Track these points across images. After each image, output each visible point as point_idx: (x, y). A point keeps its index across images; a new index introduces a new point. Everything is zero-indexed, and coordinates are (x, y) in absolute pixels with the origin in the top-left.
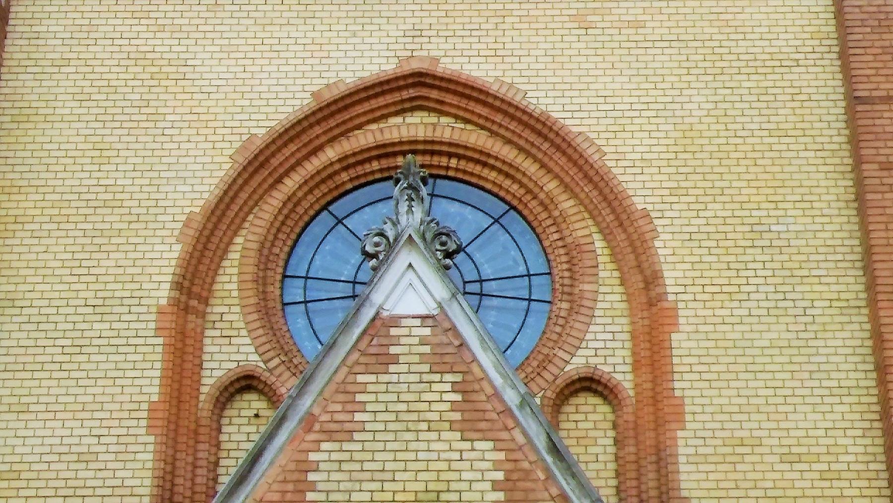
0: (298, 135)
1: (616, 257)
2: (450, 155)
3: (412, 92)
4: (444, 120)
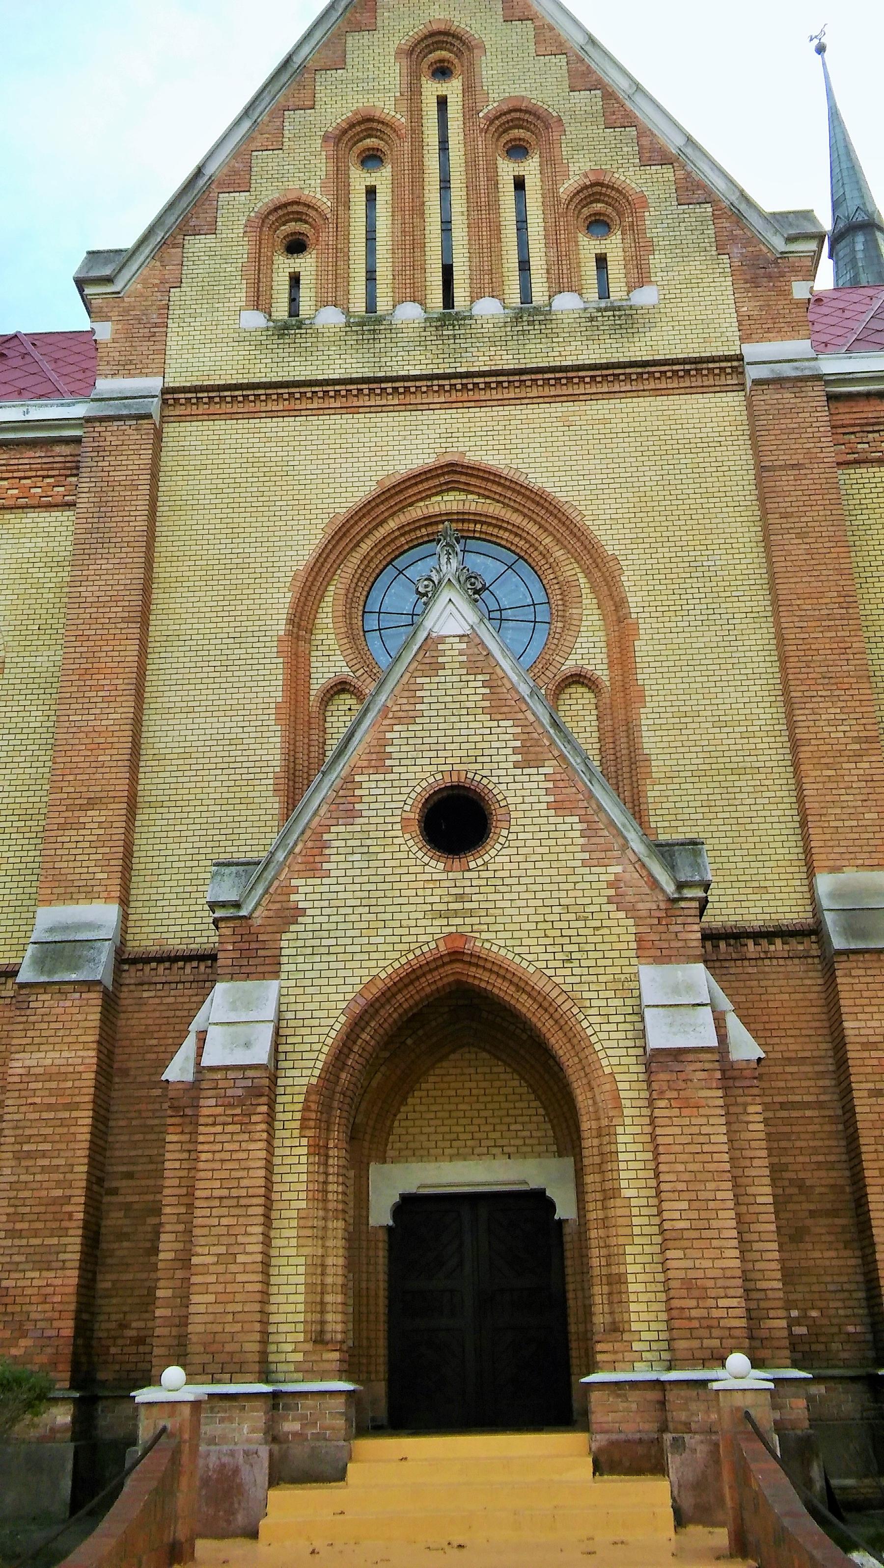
0: (369, 512)
1: (593, 589)
2: (476, 522)
3: (447, 478)
4: (470, 497)
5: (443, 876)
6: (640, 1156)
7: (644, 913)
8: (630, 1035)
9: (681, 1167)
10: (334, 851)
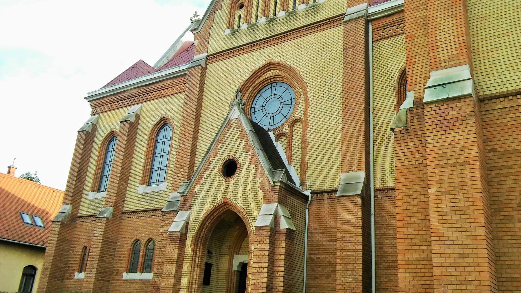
3: (269, 67)
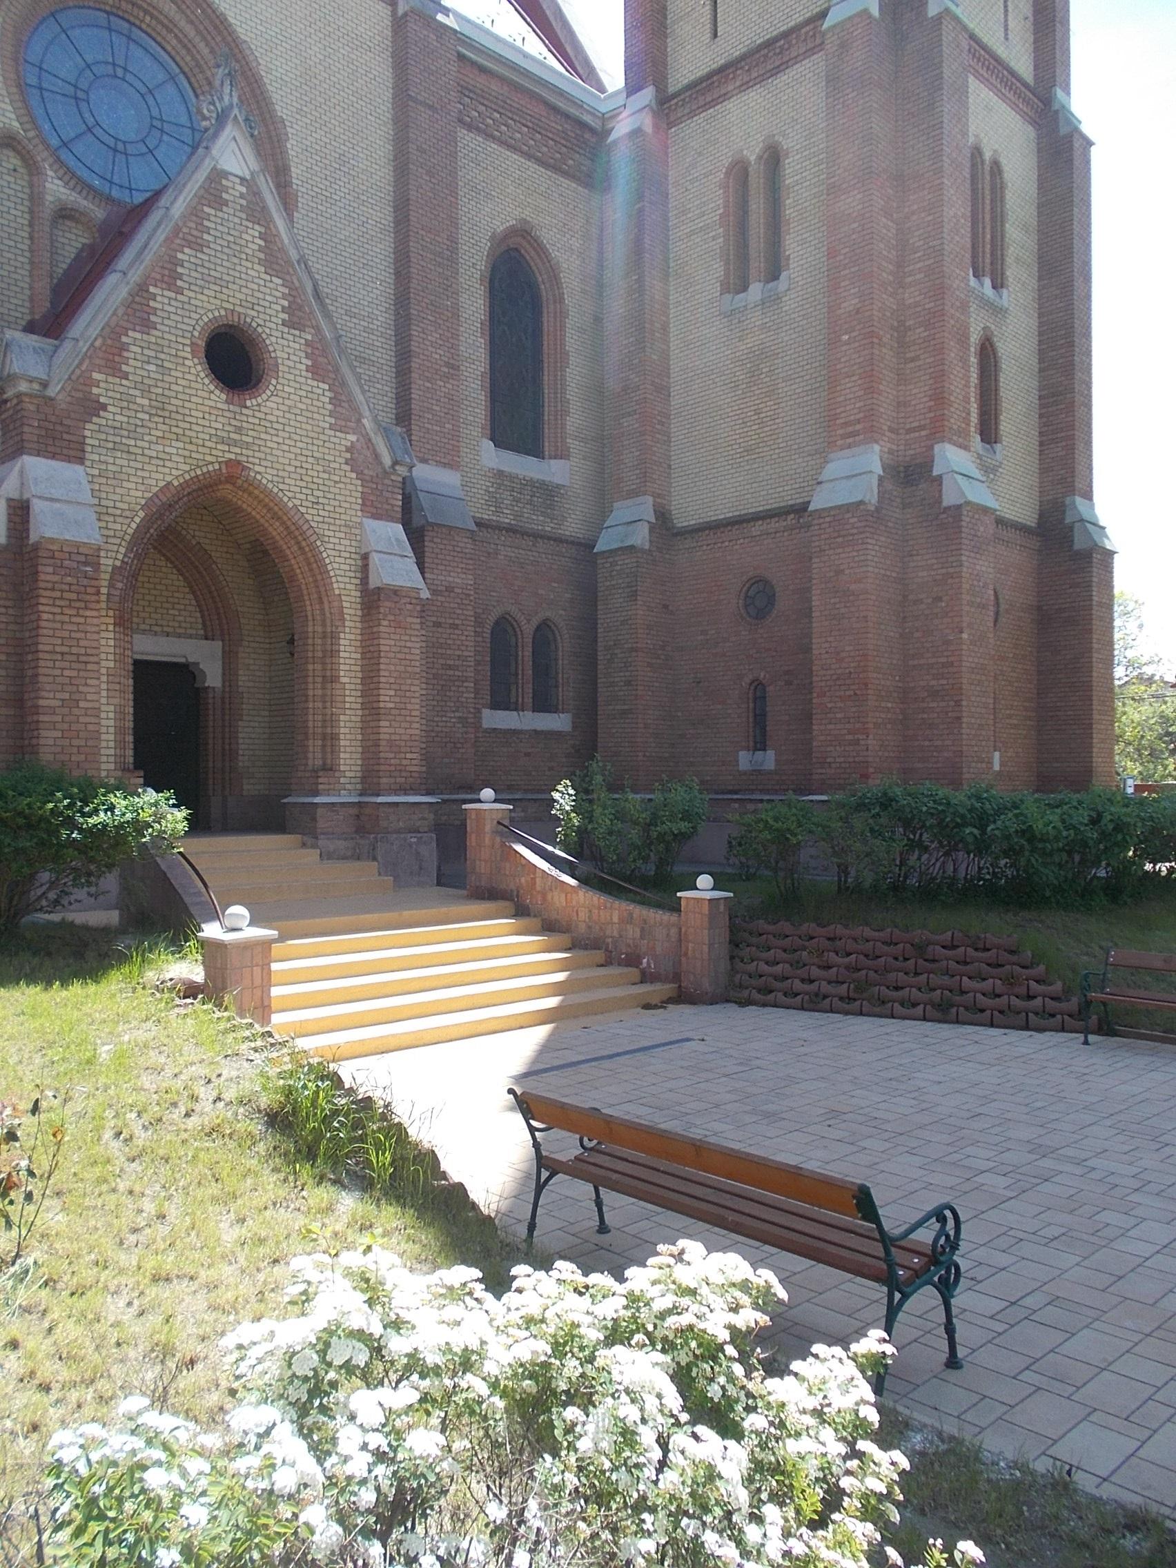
2: (146, 12)
5: (225, 407)
6: (353, 656)
7: (368, 478)
8: (353, 568)
9: (392, 668)
10: (132, 355)
